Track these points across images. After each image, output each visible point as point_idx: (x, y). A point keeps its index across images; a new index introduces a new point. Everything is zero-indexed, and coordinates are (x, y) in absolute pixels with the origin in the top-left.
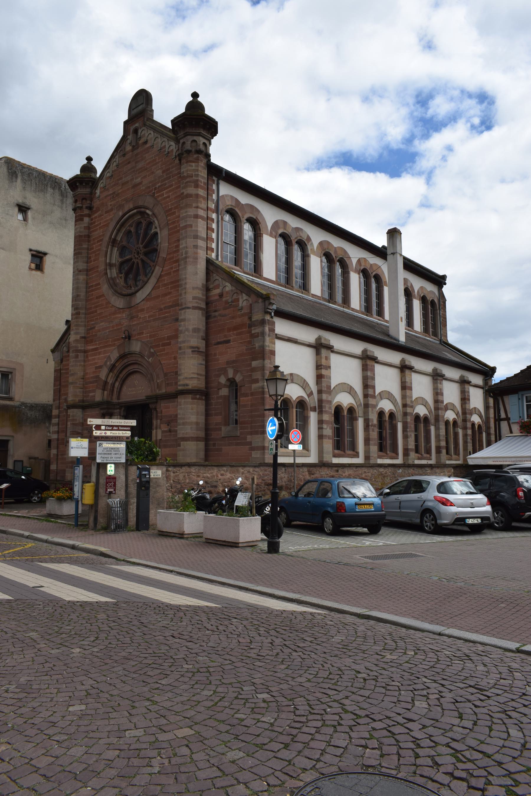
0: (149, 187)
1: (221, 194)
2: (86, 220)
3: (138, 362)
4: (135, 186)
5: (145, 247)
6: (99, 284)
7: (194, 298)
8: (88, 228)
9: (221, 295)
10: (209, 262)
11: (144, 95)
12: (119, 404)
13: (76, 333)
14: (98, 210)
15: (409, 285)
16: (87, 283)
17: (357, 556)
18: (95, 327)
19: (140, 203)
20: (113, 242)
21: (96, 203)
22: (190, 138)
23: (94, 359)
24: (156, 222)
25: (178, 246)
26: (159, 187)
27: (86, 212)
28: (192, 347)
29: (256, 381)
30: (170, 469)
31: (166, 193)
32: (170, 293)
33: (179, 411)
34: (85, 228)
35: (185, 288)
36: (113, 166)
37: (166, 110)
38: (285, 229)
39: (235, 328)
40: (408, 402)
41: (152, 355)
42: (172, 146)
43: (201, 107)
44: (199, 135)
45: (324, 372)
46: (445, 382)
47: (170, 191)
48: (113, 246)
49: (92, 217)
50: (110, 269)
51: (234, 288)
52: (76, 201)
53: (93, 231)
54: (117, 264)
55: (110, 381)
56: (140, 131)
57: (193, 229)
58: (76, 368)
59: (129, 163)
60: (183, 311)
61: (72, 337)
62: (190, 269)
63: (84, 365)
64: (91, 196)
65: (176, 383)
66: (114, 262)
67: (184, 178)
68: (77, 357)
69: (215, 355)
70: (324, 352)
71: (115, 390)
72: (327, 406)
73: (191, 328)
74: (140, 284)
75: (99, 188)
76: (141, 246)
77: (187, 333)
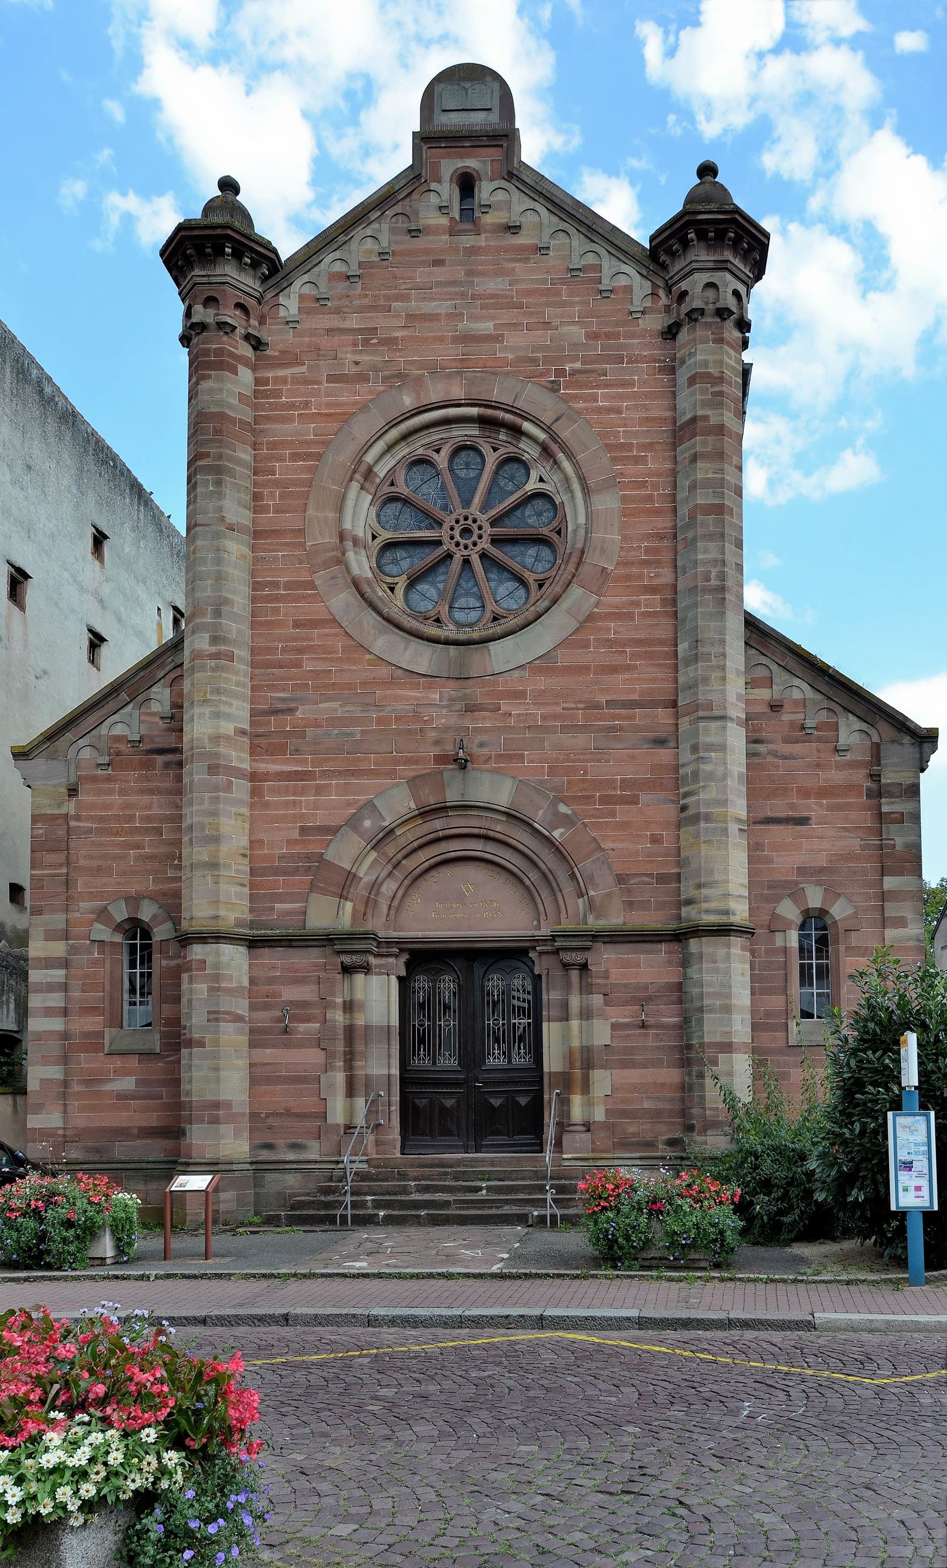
0: (534, 361)
3: (491, 834)
4: (466, 339)
14: (289, 358)
18: (291, 711)
19: (496, 394)
21: (277, 338)
26: (574, 372)
36: (361, 248)
47: (621, 397)
53: (268, 419)
66: (360, 533)
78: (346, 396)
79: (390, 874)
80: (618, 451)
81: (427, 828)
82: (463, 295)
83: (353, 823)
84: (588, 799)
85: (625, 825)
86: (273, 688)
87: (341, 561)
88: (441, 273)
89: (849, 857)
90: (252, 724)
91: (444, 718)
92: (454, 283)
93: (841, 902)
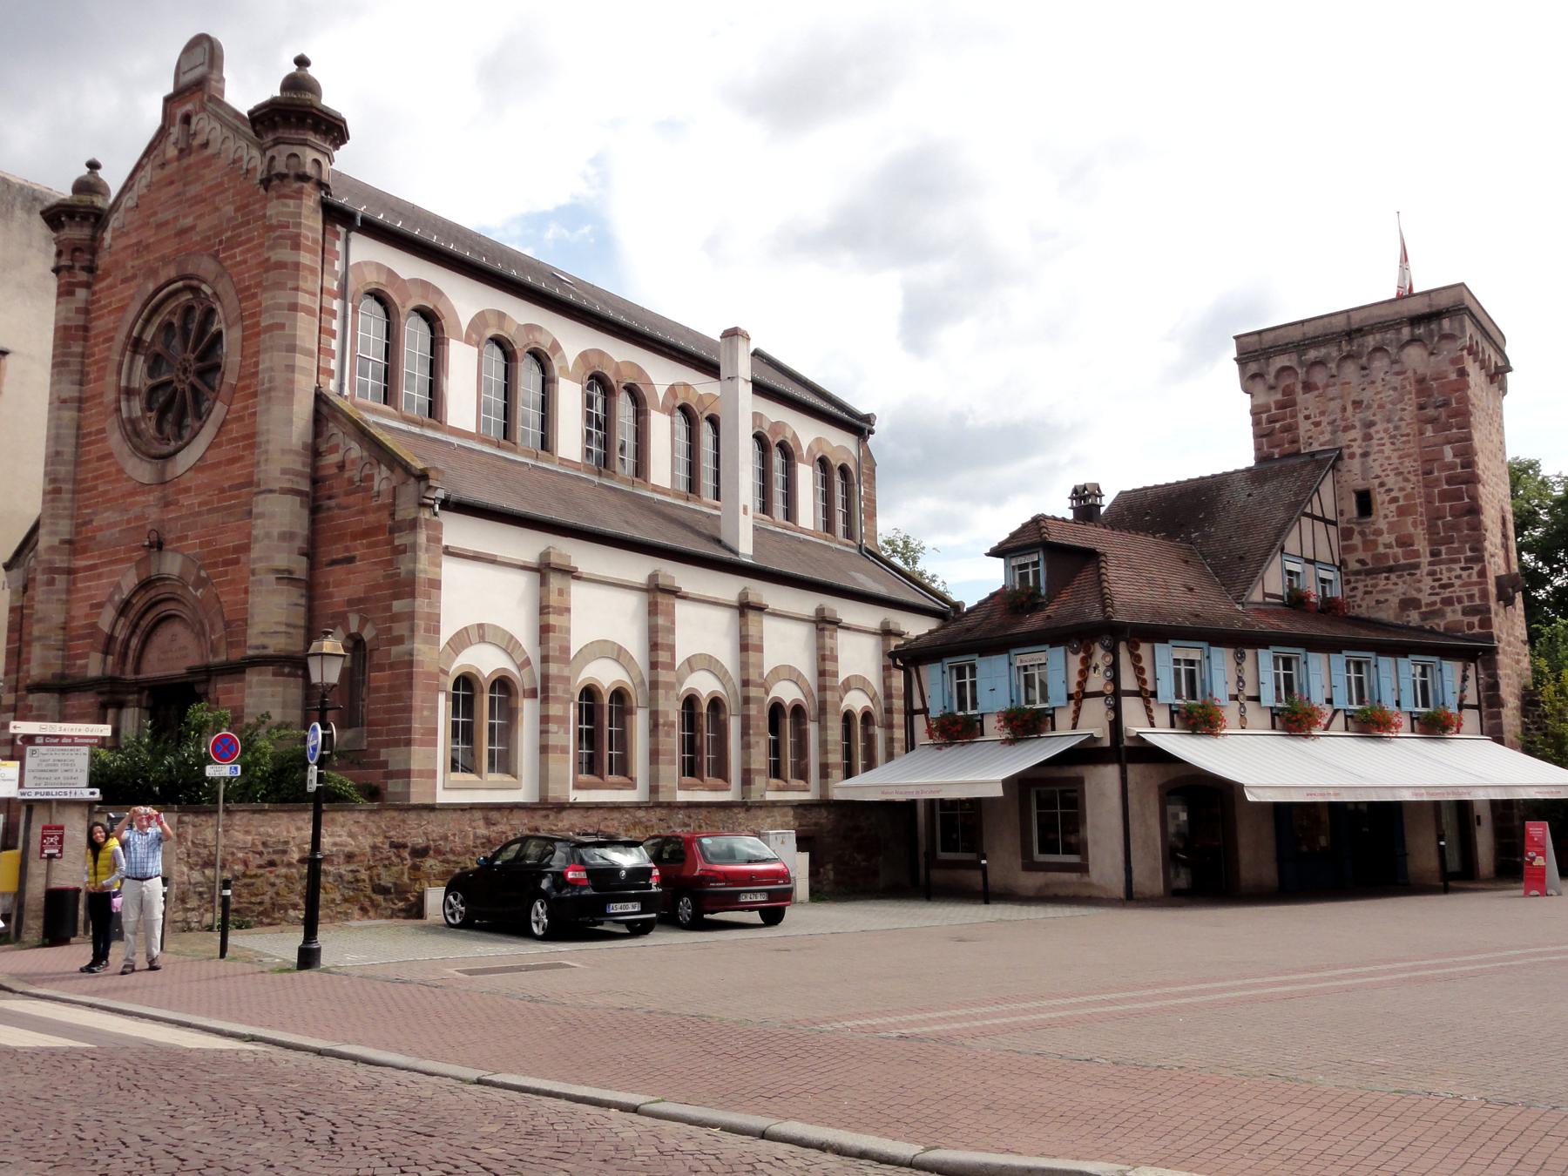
0: (208, 238)
1: (351, 263)
2: (81, 294)
4: (183, 232)
5: (200, 359)
6: (103, 431)
7: (284, 472)
8: (86, 311)
9: (341, 466)
10: (320, 398)
11: (207, 45)
12: (137, 682)
13: (53, 533)
14: (107, 274)
15: (789, 435)
16: (79, 428)
17: (451, 971)
18: (91, 521)
19: (190, 269)
20: (136, 344)
21: (103, 260)
22: (287, 149)
23: (89, 588)
24: (219, 310)
25: (256, 364)
27: (83, 276)
28: (277, 571)
29: (399, 640)
30: (186, 819)
31: (242, 253)
32: (241, 458)
33: (247, 700)
34: (78, 310)
35: (266, 452)
37: (247, 88)
38: (501, 327)
39: (366, 533)
40: (753, 676)
41: (201, 583)
42: (255, 160)
43: (312, 87)
44: (304, 143)
45: (553, 619)
46: (841, 635)
47: (249, 250)
48: (135, 352)
49: (97, 288)
50: (128, 400)
51: (365, 454)
52: (59, 254)
54: (144, 390)
55: (121, 634)
56: (194, 120)
57: (287, 331)
58: (48, 608)
59: (172, 183)
60: (261, 497)
61: (44, 540)
62: (277, 411)
63: (68, 601)
64: (93, 246)
65: (242, 644)
67: (271, 228)
68: (51, 582)
69: (327, 585)
70: (555, 581)
71: (131, 654)
72: (560, 687)
73: (275, 532)
74: (187, 434)
75: (110, 229)
76: (192, 357)
77: (266, 542)
78: (128, 290)
79: (133, 633)
80: (245, 293)
81: (148, 596)
82: (180, 202)
83: (111, 598)
84: (215, 565)
85: (231, 582)
86: (86, 507)
87: (118, 410)
88: (172, 190)
89: (377, 587)
90: (78, 533)
91: (154, 514)
92: (178, 195)
93: (369, 626)
